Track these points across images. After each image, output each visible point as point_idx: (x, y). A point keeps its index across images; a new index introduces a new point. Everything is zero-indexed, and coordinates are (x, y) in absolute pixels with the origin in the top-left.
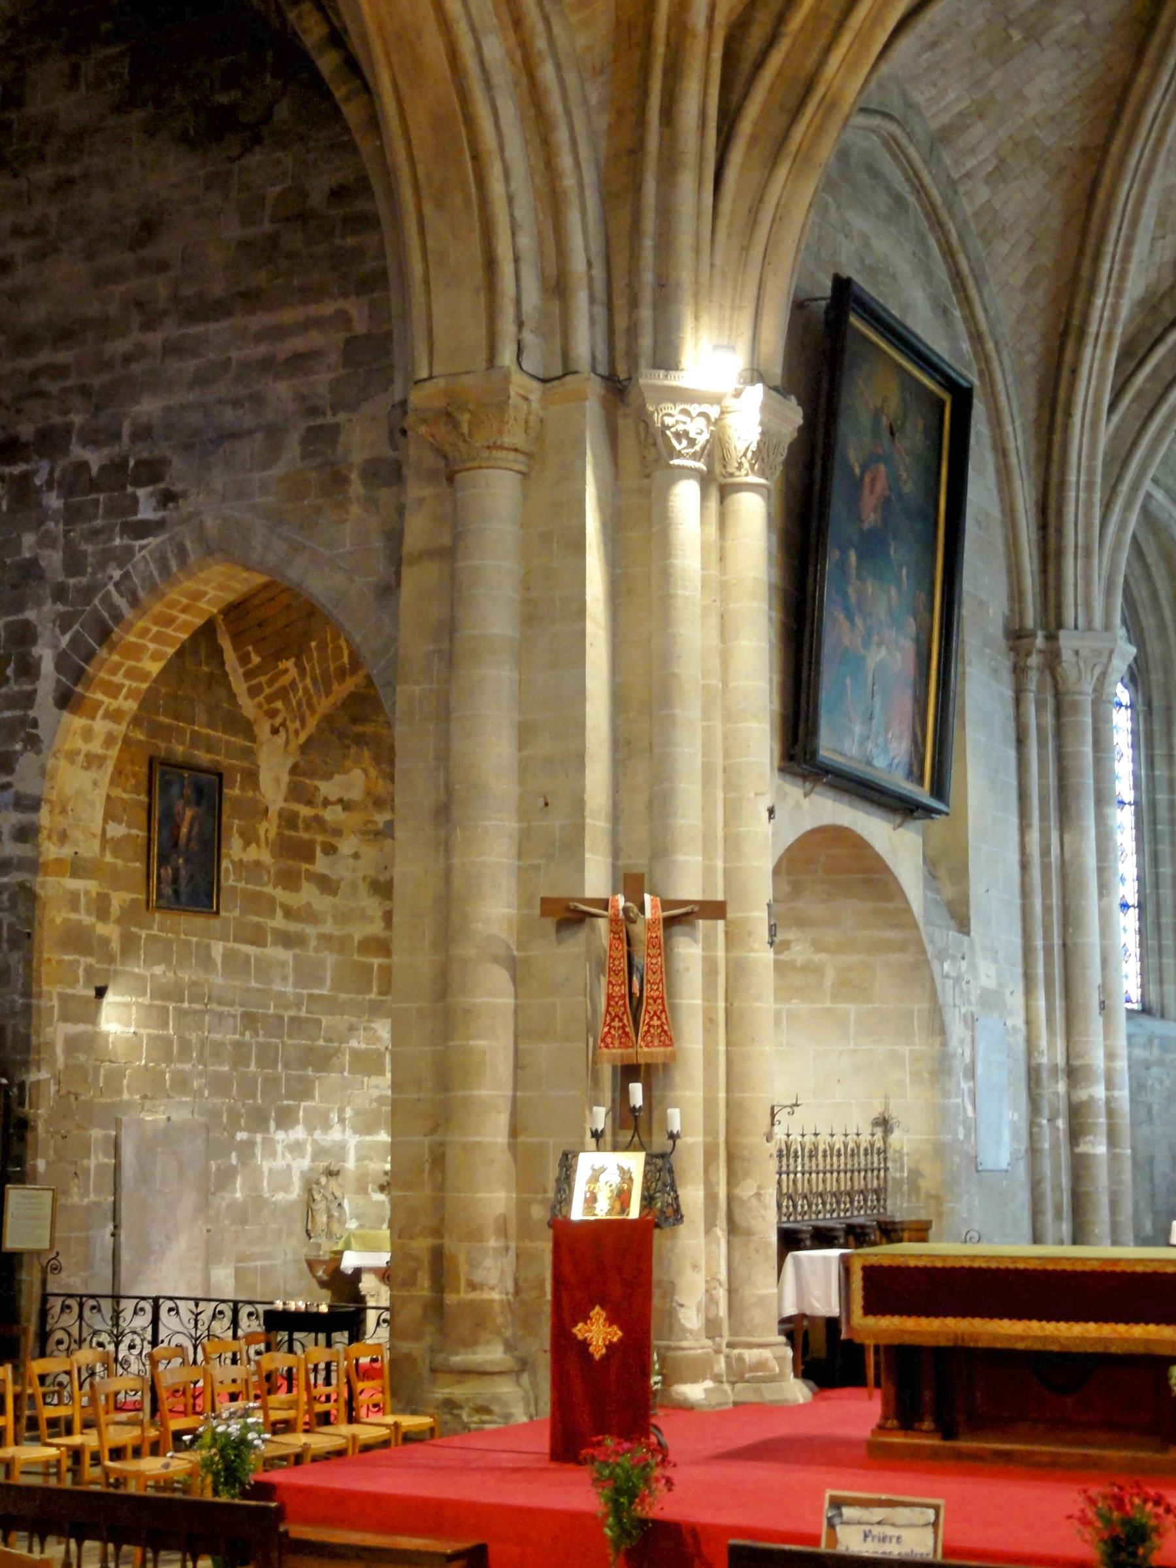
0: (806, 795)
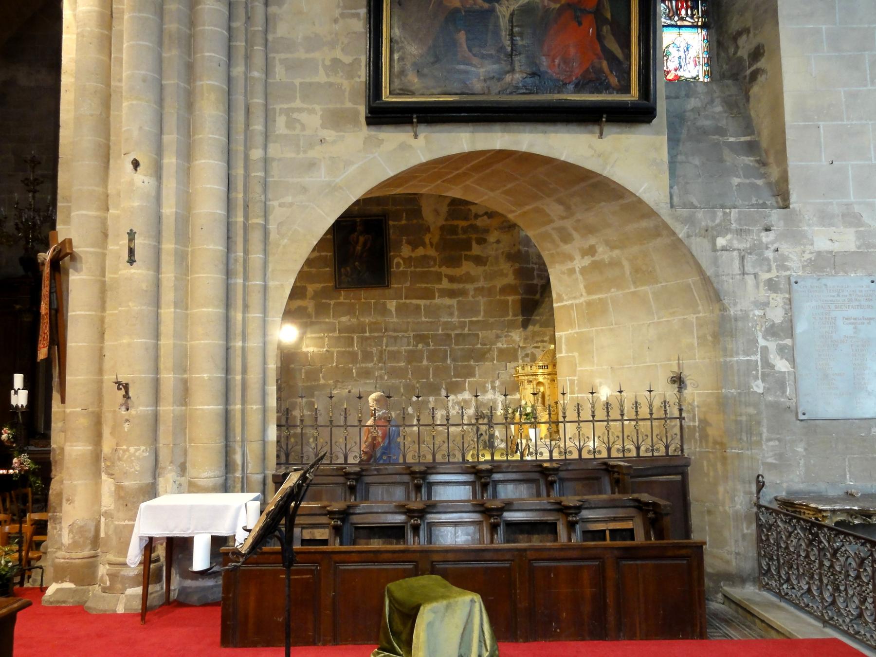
0: (416, 136)
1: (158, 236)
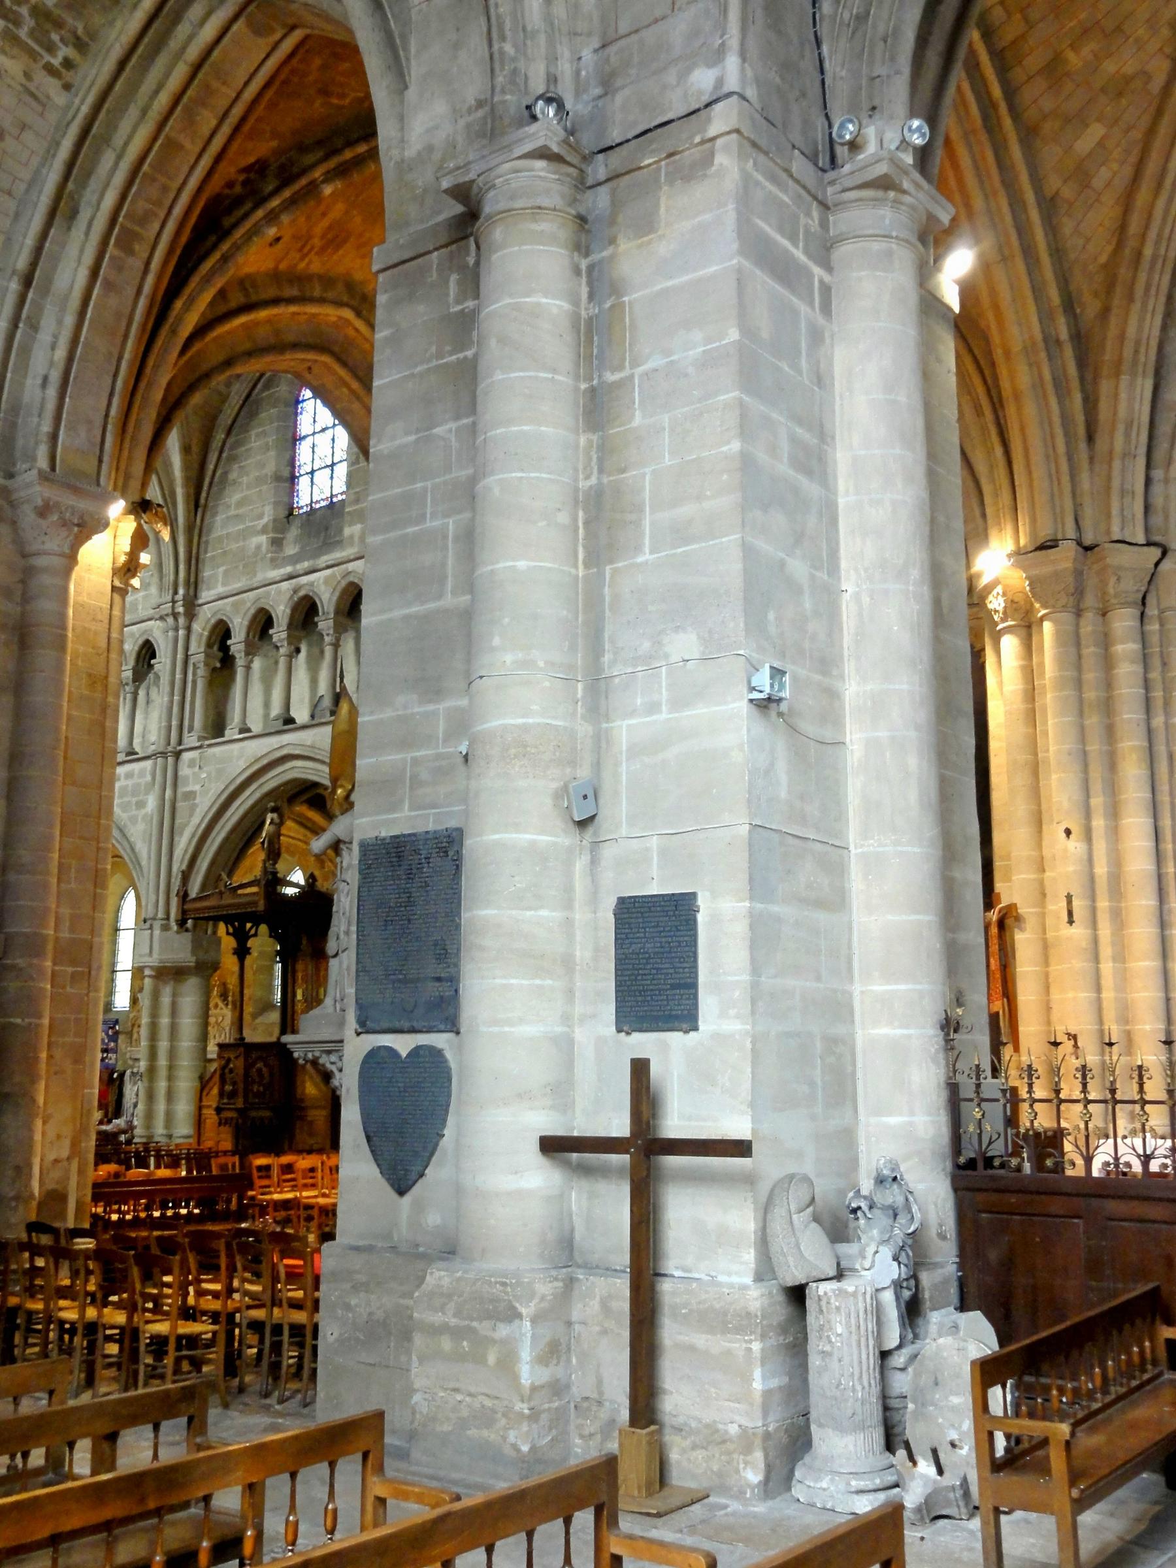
1: (1093, 898)
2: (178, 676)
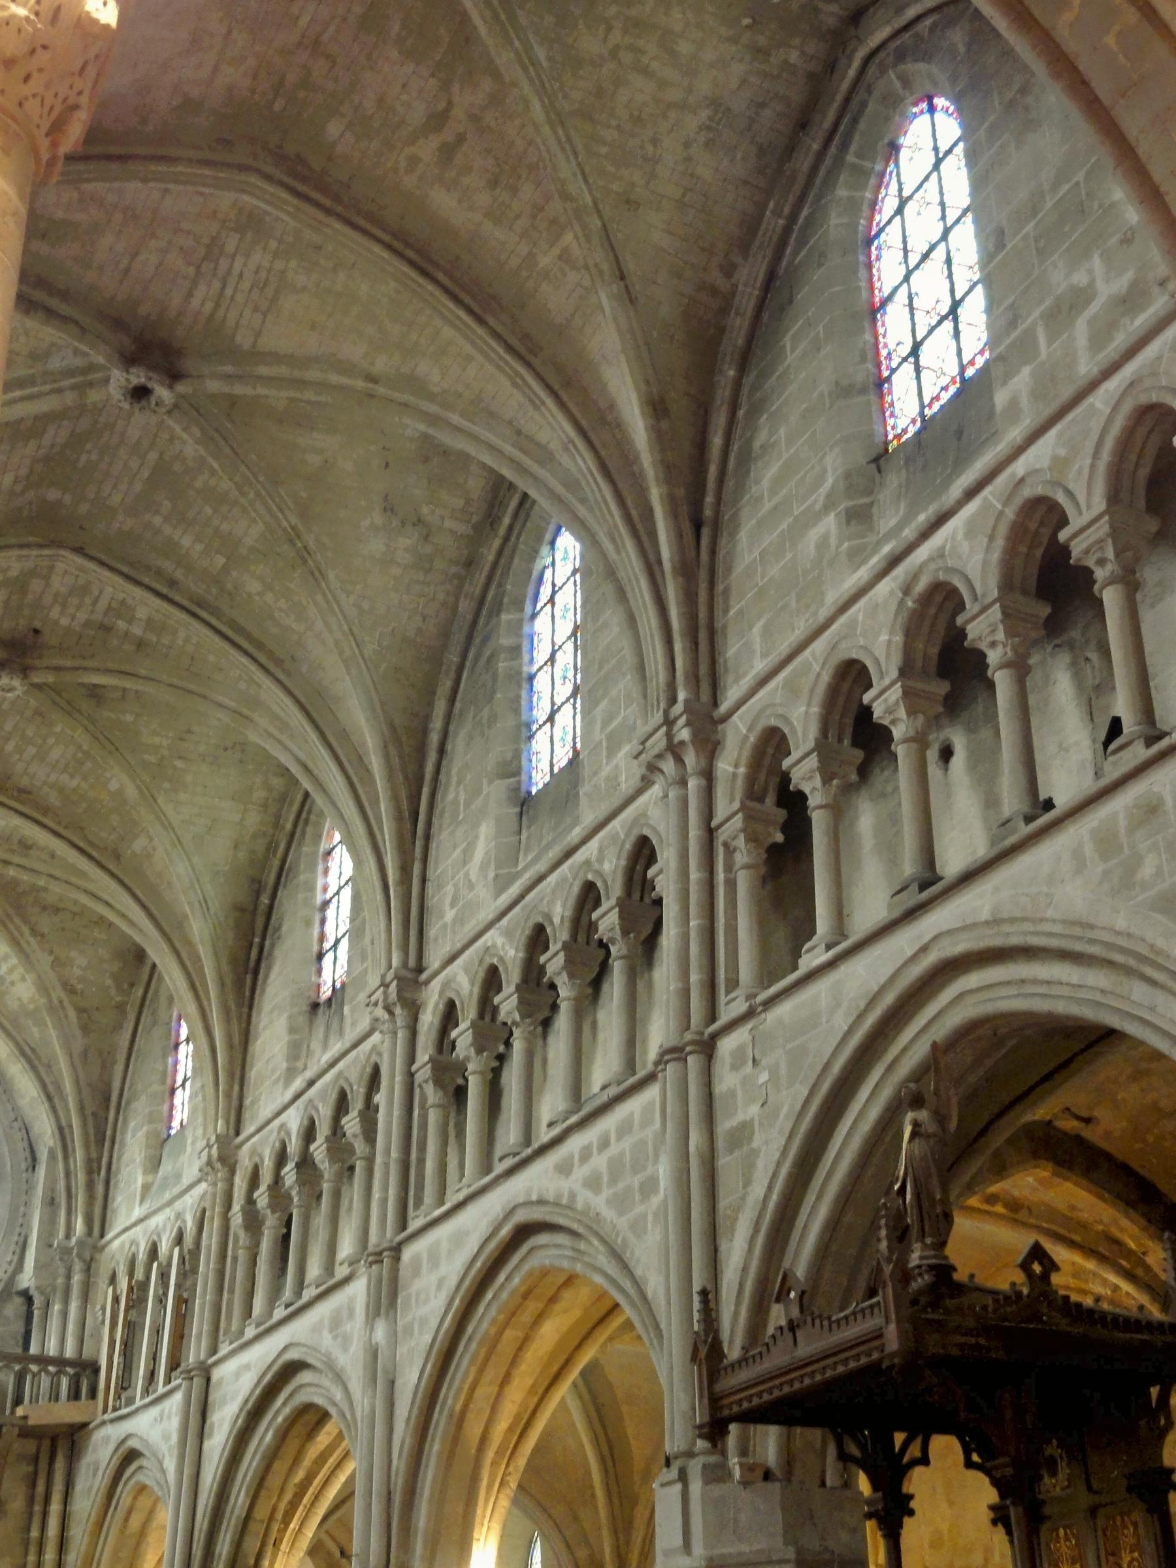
2: (695, 875)
